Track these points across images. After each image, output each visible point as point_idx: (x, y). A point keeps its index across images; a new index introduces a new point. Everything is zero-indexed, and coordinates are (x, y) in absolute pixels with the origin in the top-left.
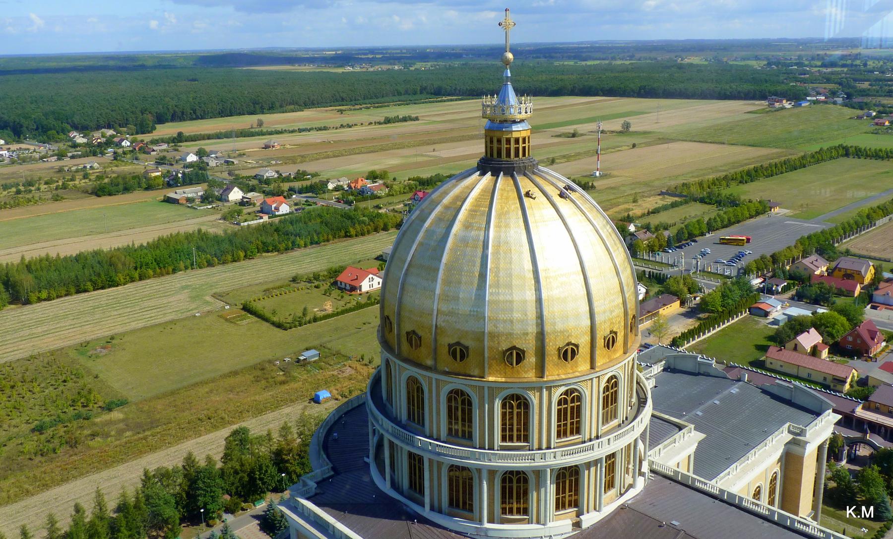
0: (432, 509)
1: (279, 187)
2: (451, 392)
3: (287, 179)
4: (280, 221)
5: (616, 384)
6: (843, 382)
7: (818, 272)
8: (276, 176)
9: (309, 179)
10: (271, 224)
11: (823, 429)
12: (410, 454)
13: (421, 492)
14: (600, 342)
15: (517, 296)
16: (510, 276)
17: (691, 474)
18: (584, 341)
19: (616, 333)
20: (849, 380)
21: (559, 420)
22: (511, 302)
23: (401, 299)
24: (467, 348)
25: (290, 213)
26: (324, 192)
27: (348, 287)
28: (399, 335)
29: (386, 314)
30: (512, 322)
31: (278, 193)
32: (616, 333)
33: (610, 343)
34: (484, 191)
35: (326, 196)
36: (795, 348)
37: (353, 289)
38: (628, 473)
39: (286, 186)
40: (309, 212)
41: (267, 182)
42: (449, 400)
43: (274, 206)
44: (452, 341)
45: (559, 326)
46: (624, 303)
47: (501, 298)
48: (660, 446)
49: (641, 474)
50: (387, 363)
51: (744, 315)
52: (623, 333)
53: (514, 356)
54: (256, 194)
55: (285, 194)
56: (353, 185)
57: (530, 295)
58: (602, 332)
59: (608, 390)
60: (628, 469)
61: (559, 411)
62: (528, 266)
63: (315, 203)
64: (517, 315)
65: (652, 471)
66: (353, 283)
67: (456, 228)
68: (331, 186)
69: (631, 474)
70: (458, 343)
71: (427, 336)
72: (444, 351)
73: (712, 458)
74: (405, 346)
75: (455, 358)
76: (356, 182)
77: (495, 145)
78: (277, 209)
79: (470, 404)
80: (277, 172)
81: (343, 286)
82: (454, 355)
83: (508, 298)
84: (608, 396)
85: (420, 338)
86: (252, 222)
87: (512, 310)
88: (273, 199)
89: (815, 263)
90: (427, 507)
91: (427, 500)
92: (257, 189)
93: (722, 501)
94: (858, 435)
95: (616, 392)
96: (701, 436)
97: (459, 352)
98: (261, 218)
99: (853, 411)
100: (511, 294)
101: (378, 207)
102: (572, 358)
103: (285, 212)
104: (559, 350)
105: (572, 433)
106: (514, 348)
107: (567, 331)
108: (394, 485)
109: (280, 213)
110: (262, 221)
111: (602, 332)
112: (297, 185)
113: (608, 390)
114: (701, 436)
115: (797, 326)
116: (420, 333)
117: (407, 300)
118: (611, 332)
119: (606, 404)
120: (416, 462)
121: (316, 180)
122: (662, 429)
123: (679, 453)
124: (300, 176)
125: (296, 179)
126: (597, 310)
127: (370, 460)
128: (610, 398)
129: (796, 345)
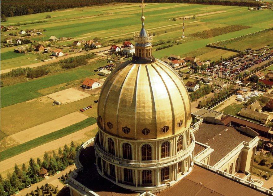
0: (119, 182)
2: (124, 144)
5: (182, 138)
6: (266, 120)
7: (260, 79)
11: (255, 142)
12: (110, 165)
13: (115, 176)
14: (176, 125)
15: (146, 111)
16: (144, 103)
17: (209, 166)
18: (170, 125)
19: (182, 121)
20: (267, 119)
21: (162, 152)
22: (144, 113)
23: (105, 112)
24: (129, 129)
27: (87, 87)
28: (104, 123)
29: (100, 115)
30: (145, 119)
32: (182, 121)
33: (180, 125)
34: (135, 70)
36: (251, 108)
37: (89, 87)
38: (186, 166)
42: (123, 147)
43: (57, 53)
44: (123, 127)
45: (162, 121)
46: (185, 110)
47: (141, 111)
48: (198, 155)
49: (191, 166)
50: (101, 132)
51: (234, 95)
52: (184, 121)
53: (146, 132)
56: (88, 43)
57: (151, 111)
58: (177, 121)
59: (179, 141)
60: (186, 165)
61: (162, 149)
62: (150, 99)
64: (147, 117)
65: (195, 164)
66: (89, 85)
67: (124, 85)
69: (187, 166)
70: (126, 127)
71: (115, 125)
72: (121, 130)
73: (214, 159)
74: (107, 128)
75: (125, 133)
76: (89, 41)
77: (139, 52)
78: (58, 54)
79: (131, 148)
81: (85, 86)
82: (124, 131)
83: (144, 111)
84: (179, 143)
85: (112, 125)
87: (145, 116)
88: (56, 50)
89: (260, 75)
90: (117, 182)
91: (117, 179)
93: (218, 174)
94: (268, 140)
95: (182, 141)
96: (212, 150)
97: (126, 130)
98: (52, 58)
99: (268, 132)
100: (145, 110)
102: (166, 131)
104: (162, 129)
105: (166, 156)
106: (146, 129)
107: (165, 122)
108: (105, 174)
111: (177, 121)
113: (179, 141)
114: (212, 150)
115: (252, 100)
116: (112, 123)
117: (107, 112)
118: (180, 121)
119: (178, 144)
120: (112, 167)
122: (199, 149)
123: (202, 158)
126: (175, 114)
127: (96, 164)
128: (180, 142)
129: (251, 107)
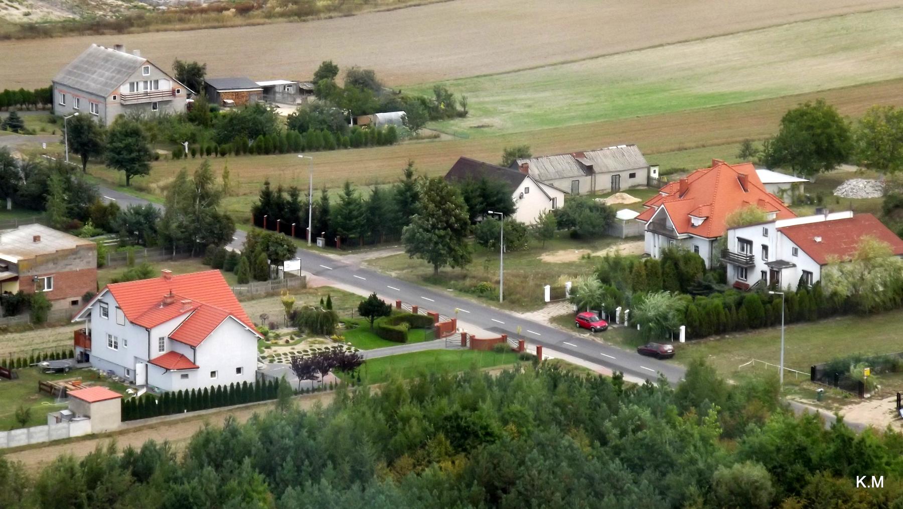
1: (203, 178)
3: (249, 133)
4: (208, 451)
8: (181, 102)
9: (387, 139)
10: (141, 467)
25: (264, 390)
26: (488, 242)
31: (195, 239)
35: (502, 270)
39: (242, 181)
40: (390, 402)
41: (127, 148)
54: (54, 241)
55: (236, 245)
63: (424, 325)
68: (531, 205)
80: (191, 77)
86: (20, 436)
92: (58, 200)
98: (82, 410)
101: (837, 378)
103: (227, 379)
109: (199, 381)
110: (80, 428)
112: (322, 176)
121: (429, 158)
124: (344, 110)
125: (304, 136)
